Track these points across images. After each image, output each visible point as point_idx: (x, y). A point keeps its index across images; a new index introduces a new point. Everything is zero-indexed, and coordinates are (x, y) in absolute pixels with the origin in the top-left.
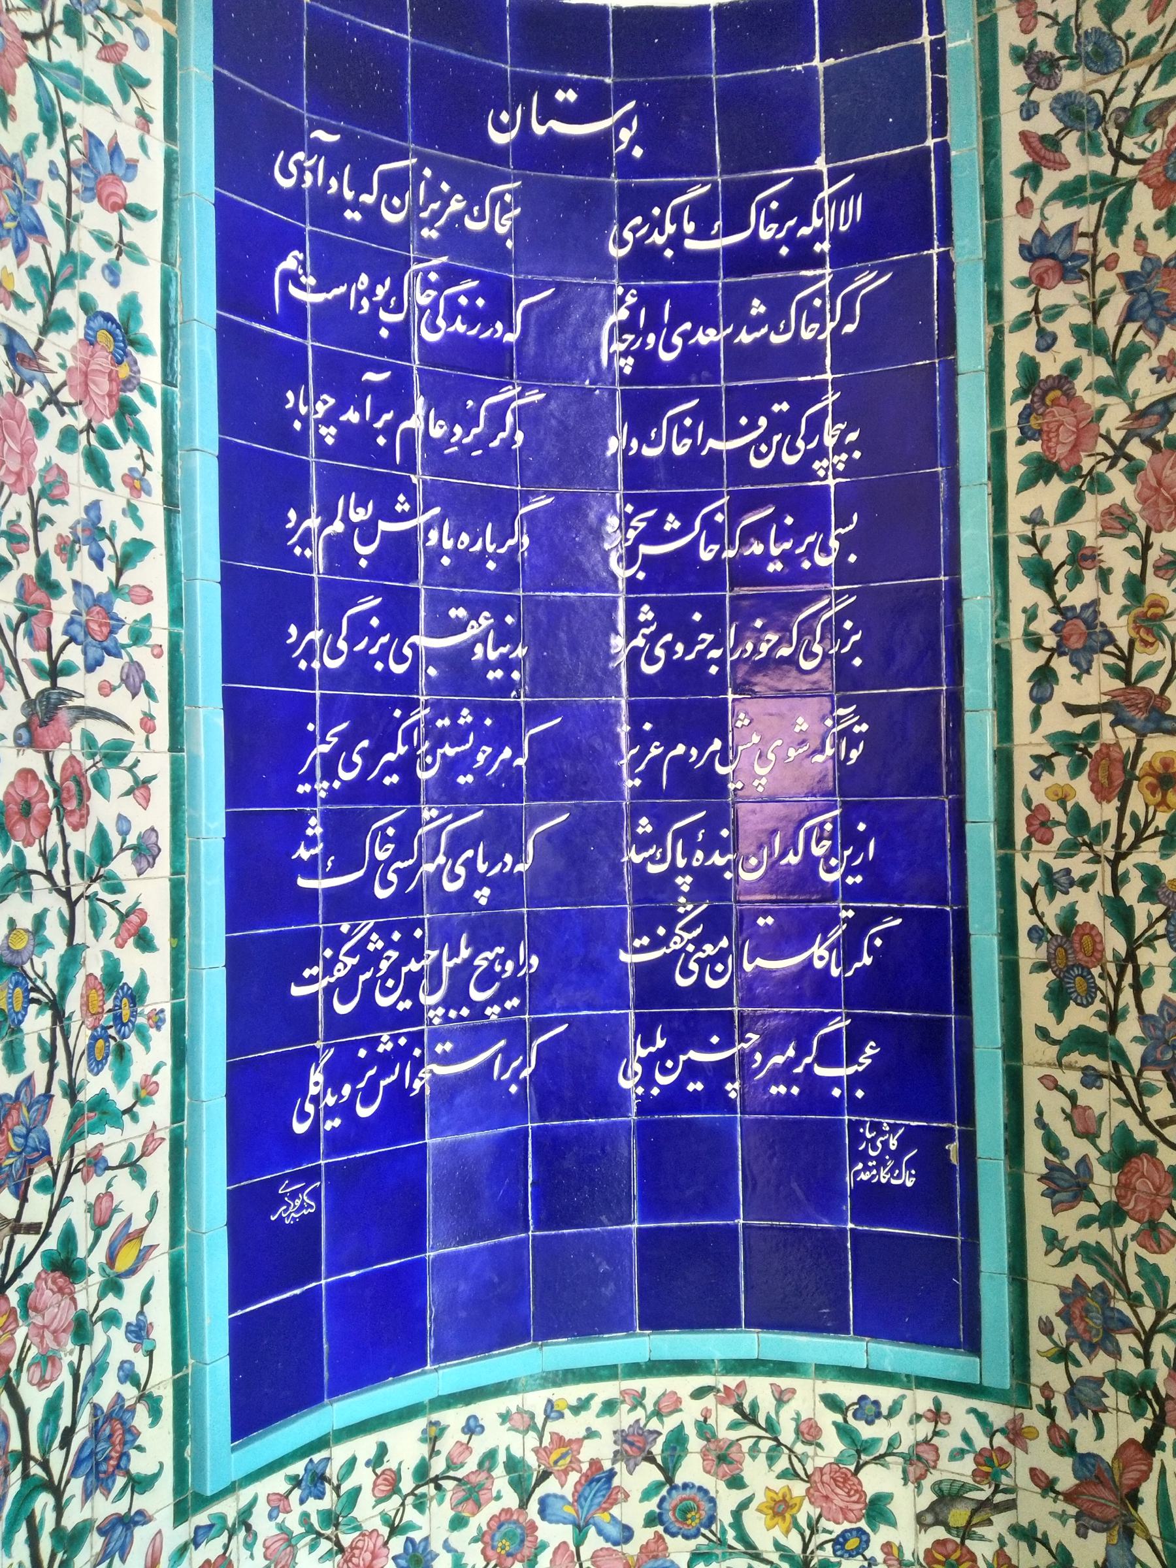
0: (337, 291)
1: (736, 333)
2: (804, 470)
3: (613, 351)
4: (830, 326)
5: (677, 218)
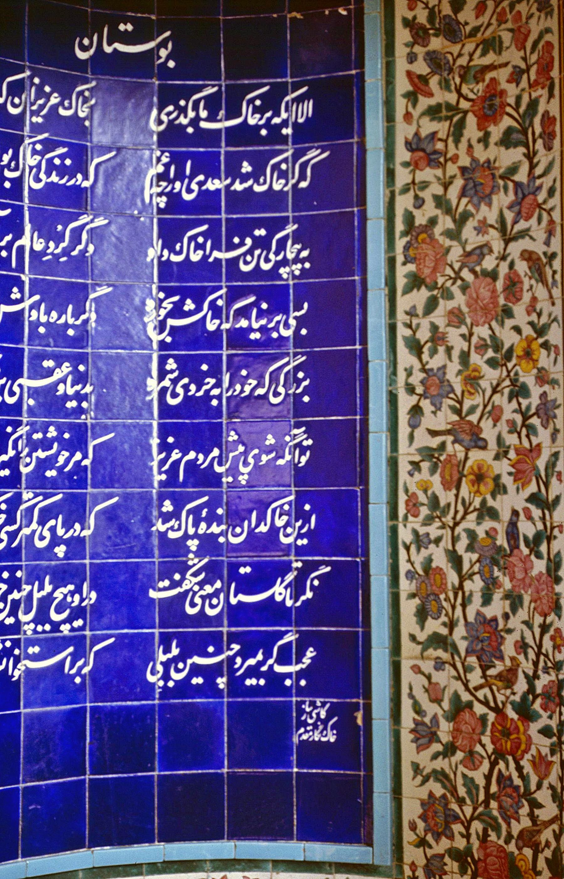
1: (232, 183)
2: (274, 273)
3: (152, 194)
4: (292, 182)
5: (196, 108)
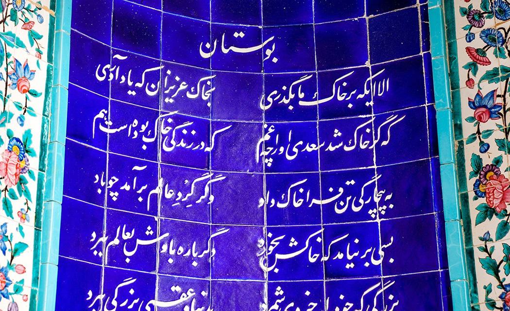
0: (122, 128)
1: (326, 146)
2: (364, 214)
3: (262, 155)
4: (375, 142)
5: (295, 91)
